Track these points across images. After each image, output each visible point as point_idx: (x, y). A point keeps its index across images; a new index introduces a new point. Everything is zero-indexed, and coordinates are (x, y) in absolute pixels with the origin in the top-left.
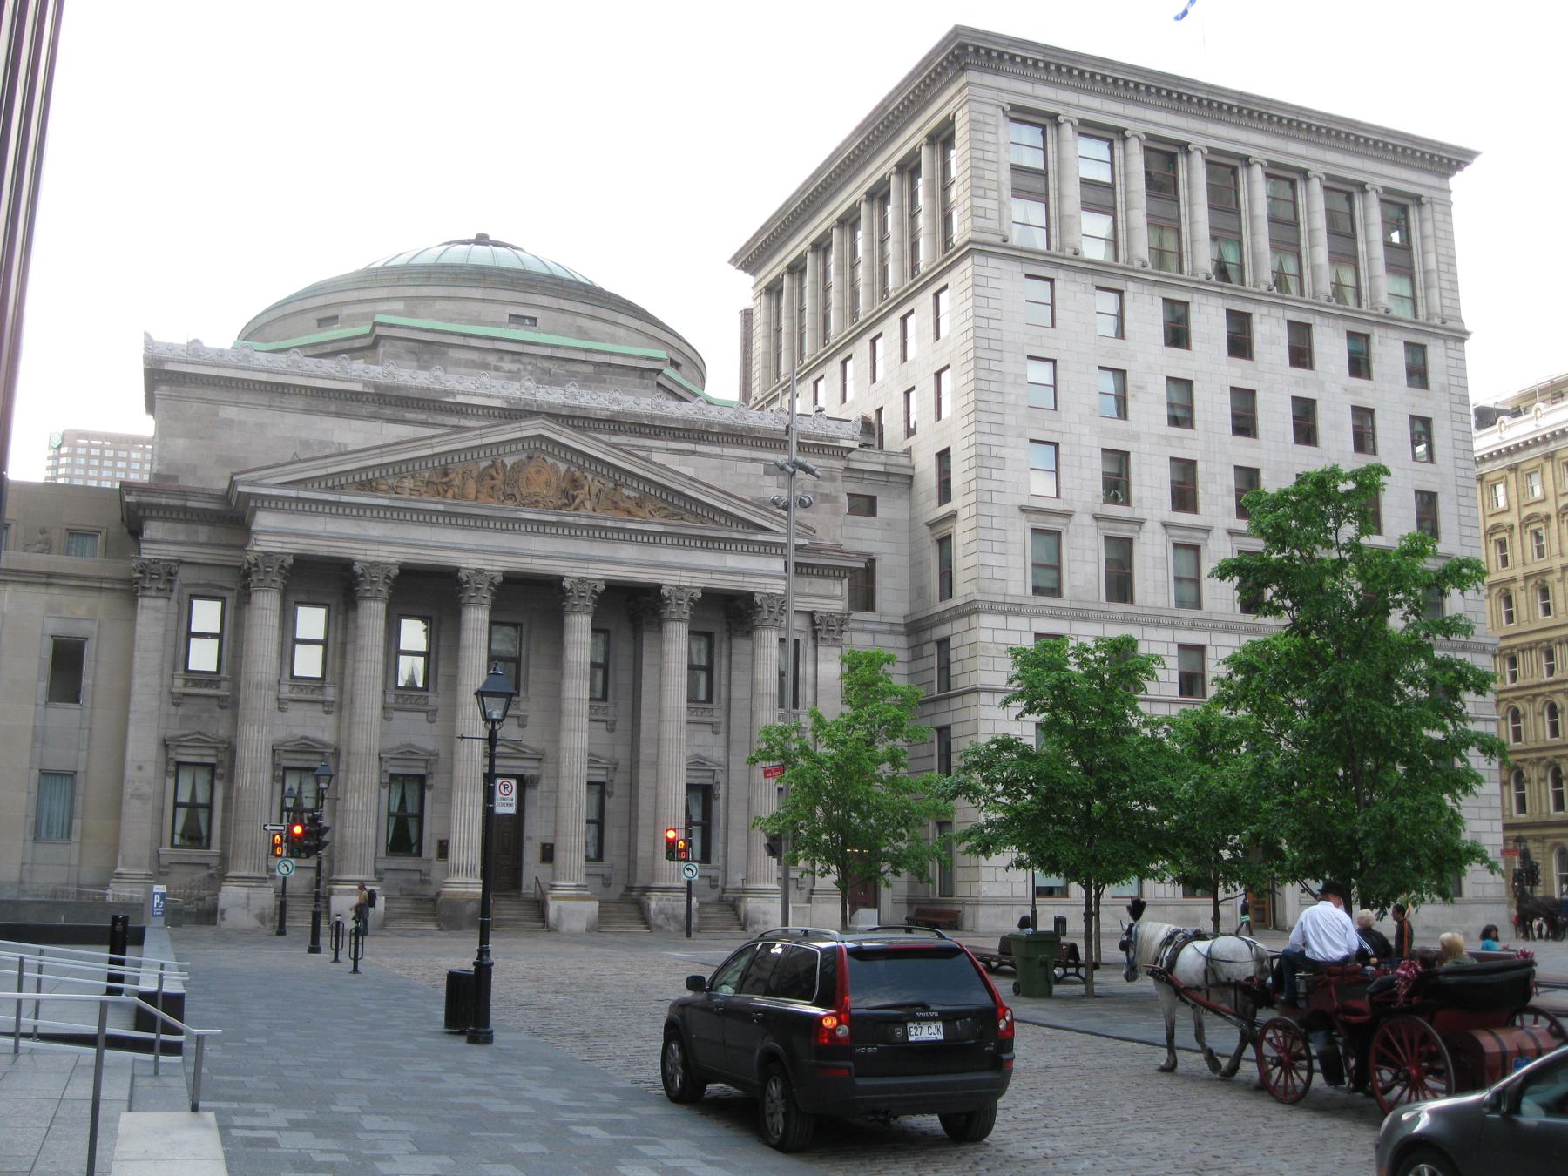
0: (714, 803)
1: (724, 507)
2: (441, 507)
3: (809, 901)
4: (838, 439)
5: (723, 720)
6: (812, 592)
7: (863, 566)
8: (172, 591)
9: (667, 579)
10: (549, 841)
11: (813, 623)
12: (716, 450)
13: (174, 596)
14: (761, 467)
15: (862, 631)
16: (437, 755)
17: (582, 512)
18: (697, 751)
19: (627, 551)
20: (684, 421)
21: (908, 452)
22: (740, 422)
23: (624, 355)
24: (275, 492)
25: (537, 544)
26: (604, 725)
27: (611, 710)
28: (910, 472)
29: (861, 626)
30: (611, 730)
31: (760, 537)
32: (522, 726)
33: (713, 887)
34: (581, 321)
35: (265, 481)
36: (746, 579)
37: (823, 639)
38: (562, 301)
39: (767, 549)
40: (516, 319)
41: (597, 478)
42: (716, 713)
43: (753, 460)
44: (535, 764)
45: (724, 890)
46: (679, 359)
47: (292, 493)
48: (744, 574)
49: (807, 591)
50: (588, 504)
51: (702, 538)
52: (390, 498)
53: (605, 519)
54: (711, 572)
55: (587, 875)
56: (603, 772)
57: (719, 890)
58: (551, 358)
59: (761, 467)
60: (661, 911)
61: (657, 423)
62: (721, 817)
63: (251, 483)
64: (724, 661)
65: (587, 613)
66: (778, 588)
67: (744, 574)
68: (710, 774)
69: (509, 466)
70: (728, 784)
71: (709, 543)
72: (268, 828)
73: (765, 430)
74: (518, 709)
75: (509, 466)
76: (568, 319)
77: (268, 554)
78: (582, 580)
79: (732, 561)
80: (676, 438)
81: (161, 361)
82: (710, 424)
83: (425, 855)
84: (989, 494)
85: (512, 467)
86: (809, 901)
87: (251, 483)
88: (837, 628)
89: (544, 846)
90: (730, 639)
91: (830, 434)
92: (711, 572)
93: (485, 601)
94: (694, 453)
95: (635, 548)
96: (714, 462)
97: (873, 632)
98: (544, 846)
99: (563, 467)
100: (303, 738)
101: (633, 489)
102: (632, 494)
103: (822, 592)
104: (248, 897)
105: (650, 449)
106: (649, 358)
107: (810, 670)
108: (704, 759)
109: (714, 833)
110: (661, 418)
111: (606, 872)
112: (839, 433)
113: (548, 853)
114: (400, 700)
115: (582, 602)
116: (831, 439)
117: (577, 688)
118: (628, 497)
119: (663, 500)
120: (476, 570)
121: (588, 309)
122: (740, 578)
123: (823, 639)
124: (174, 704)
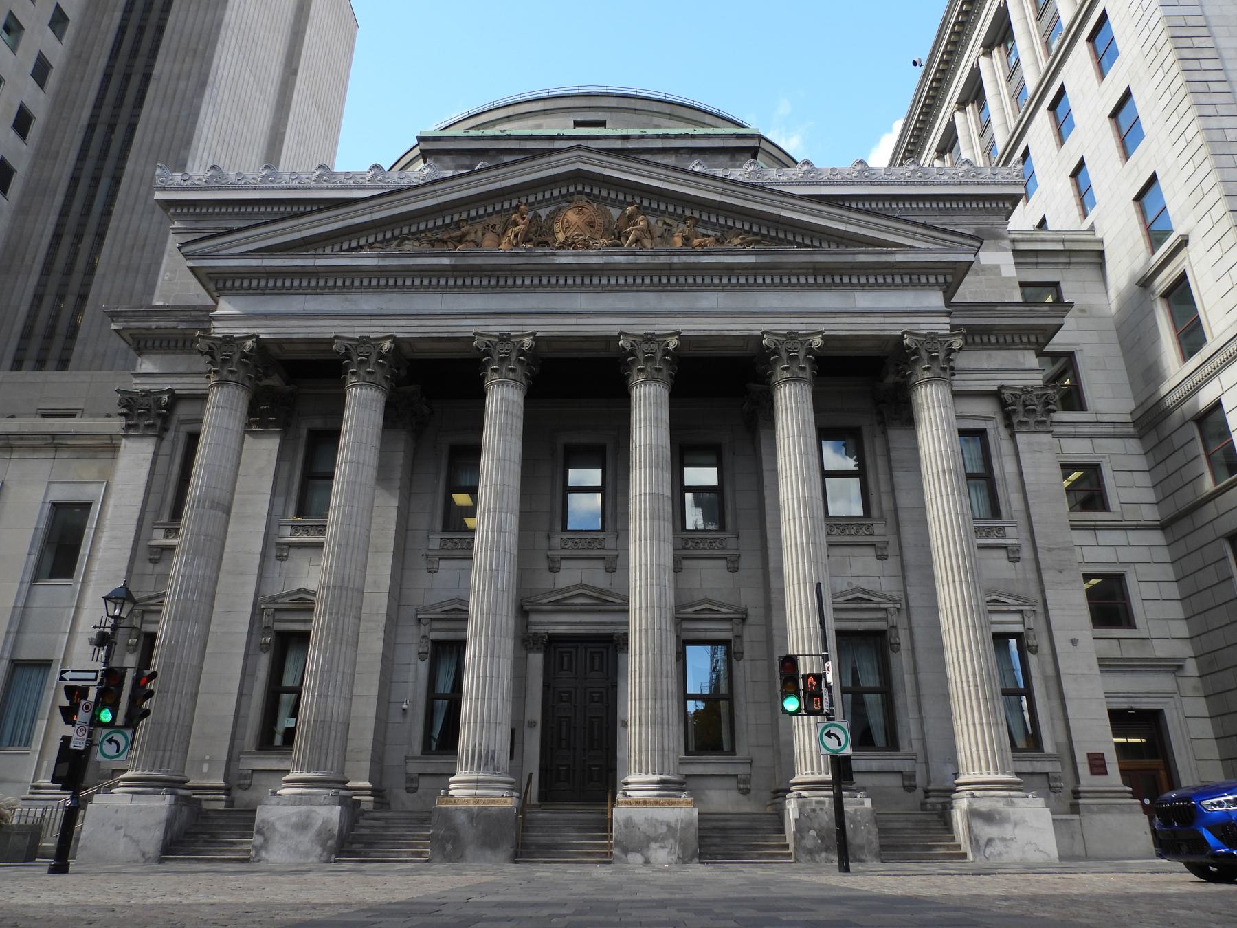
0: (893, 658)
2: (446, 261)
3: (1075, 809)
5: (892, 539)
8: (165, 429)
11: (1003, 404)
13: (170, 436)
15: (1075, 436)
18: (856, 583)
19: (709, 300)
21: (1092, 229)
25: (581, 301)
26: (723, 563)
27: (731, 543)
28: (1097, 247)
29: (1071, 429)
30: (733, 569)
31: (899, 258)
32: (611, 569)
33: (910, 788)
34: (656, 120)
37: (1021, 423)
38: (633, 101)
40: (577, 124)
41: (661, 218)
42: (878, 530)
45: (927, 792)
47: (254, 263)
49: (985, 366)
51: (816, 270)
52: (379, 256)
56: (727, 626)
57: (919, 793)
62: (908, 679)
64: (883, 478)
65: (658, 380)
68: (881, 615)
69: (543, 218)
70: (910, 628)
72: (67, 676)
74: (603, 548)
75: (543, 218)
76: (644, 118)
79: (864, 300)
85: (548, 216)
86: (1075, 809)
88: (1039, 408)
90: (884, 433)
93: (511, 375)
95: (721, 295)
97: (1091, 436)
99: (615, 212)
100: (300, 591)
101: (713, 226)
102: (710, 233)
107: (1010, 467)
108: (868, 592)
109: (899, 701)
111: (742, 770)
114: (449, 545)
119: (755, 234)
122: (880, 319)
123: (1021, 423)
124: (151, 561)
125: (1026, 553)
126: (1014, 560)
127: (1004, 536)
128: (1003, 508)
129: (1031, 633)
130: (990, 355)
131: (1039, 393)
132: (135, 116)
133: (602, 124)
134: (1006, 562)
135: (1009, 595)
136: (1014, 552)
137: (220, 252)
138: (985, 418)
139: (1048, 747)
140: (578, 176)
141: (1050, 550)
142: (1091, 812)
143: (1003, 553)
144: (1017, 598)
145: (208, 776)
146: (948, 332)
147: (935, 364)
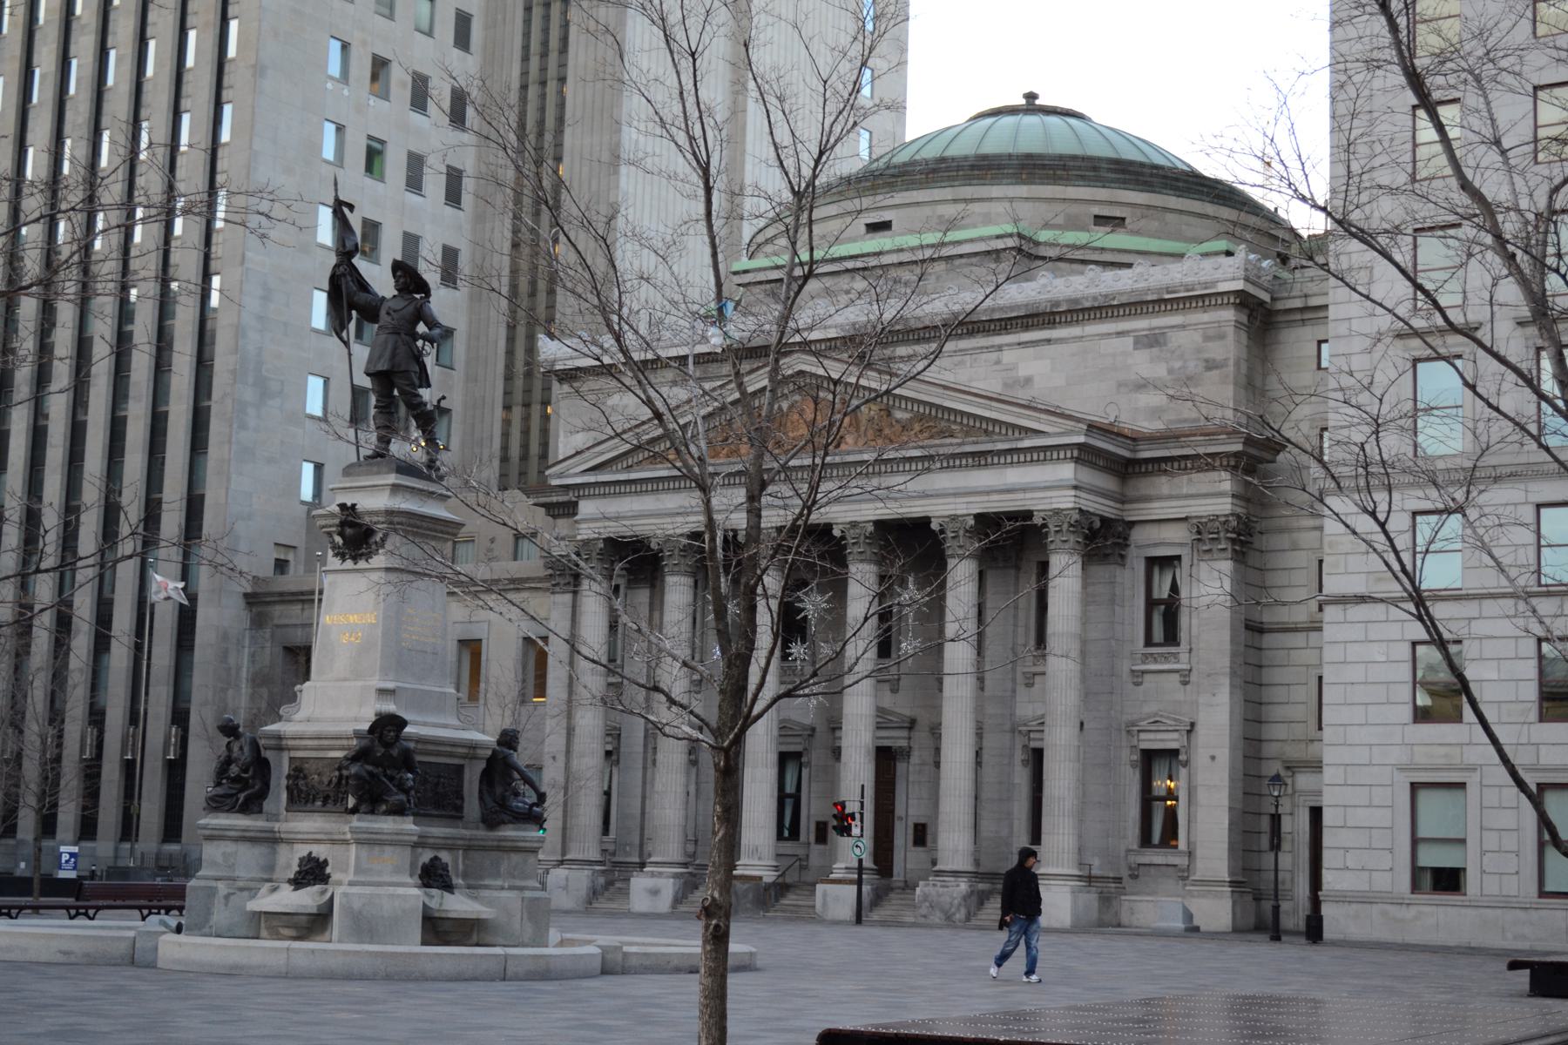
1: (987, 414)
4: (1214, 283)
6: (1193, 491)
7: (1239, 447)
9: (937, 510)
10: (922, 821)
12: (1075, 331)
14: (1129, 341)
16: (813, 729)
17: (843, 447)
20: (1027, 305)
22: (1093, 291)
23: (972, 241)
24: (579, 480)
31: (1027, 443)
32: (894, 691)
35: (571, 471)
36: (1028, 495)
39: (1045, 454)
43: (1120, 334)
44: (904, 733)
46: (1117, 213)
47: (591, 478)
48: (1024, 490)
49: (1184, 491)
50: (849, 439)
53: (861, 452)
54: (988, 493)
55: (778, 855)
58: (901, 264)
59: (1129, 341)
60: (926, 897)
61: (997, 316)
63: (560, 475)
65: (862, 561)
66: (1065, 501)
67: (1024, 490)
71: (980, 459)
73: (1121, 294)
76: (926, 211)
77: (586, 542)
78: (854, 524)
79: (1014, 475)
80: (1027, 328)
81: (554, 362)
82: (1057, 303)
83: (803, 837)
84: (1346, 324)
87: (560, 475)
89: (916, 825)
91: (1203, 279)
92: (988, 493)
94: (1048, 341)
96: (1074, 347)
98: (916, 825)
103: (1204, 489)
104: (567, 879)
105: (1000, 348)
106: (998, 237)
110: (1001, 309)
112: (1218, 275)
113: (921, 835)
115: (856, 549)
116: (1206, 285)
117: (860, 649)
118: (897, 421)
120: (851, 523)
121: (947, 193)
122: (1021, 496)
125: (1193, 678)
126: (1185, 683)
127: (1178, 662)
128: (1183, 635)
129: (1183, 750)
130: (1190, 480)
131: (1223, 519)
132: (563, 65)
133: (885, 226)
134: (1178, 685)
135: (1168, 718)
136: (1185, 676)
137: (571, 471)
138: (1181, 545)
139: (1182, 843)
140: (801, 373)
141: (1209, 675)
142: (1193, 896)
143: (1176, 677)
144: (1175, 720)
145: (630, 855)
146: (1071, 505)
147: (1059, 536)
